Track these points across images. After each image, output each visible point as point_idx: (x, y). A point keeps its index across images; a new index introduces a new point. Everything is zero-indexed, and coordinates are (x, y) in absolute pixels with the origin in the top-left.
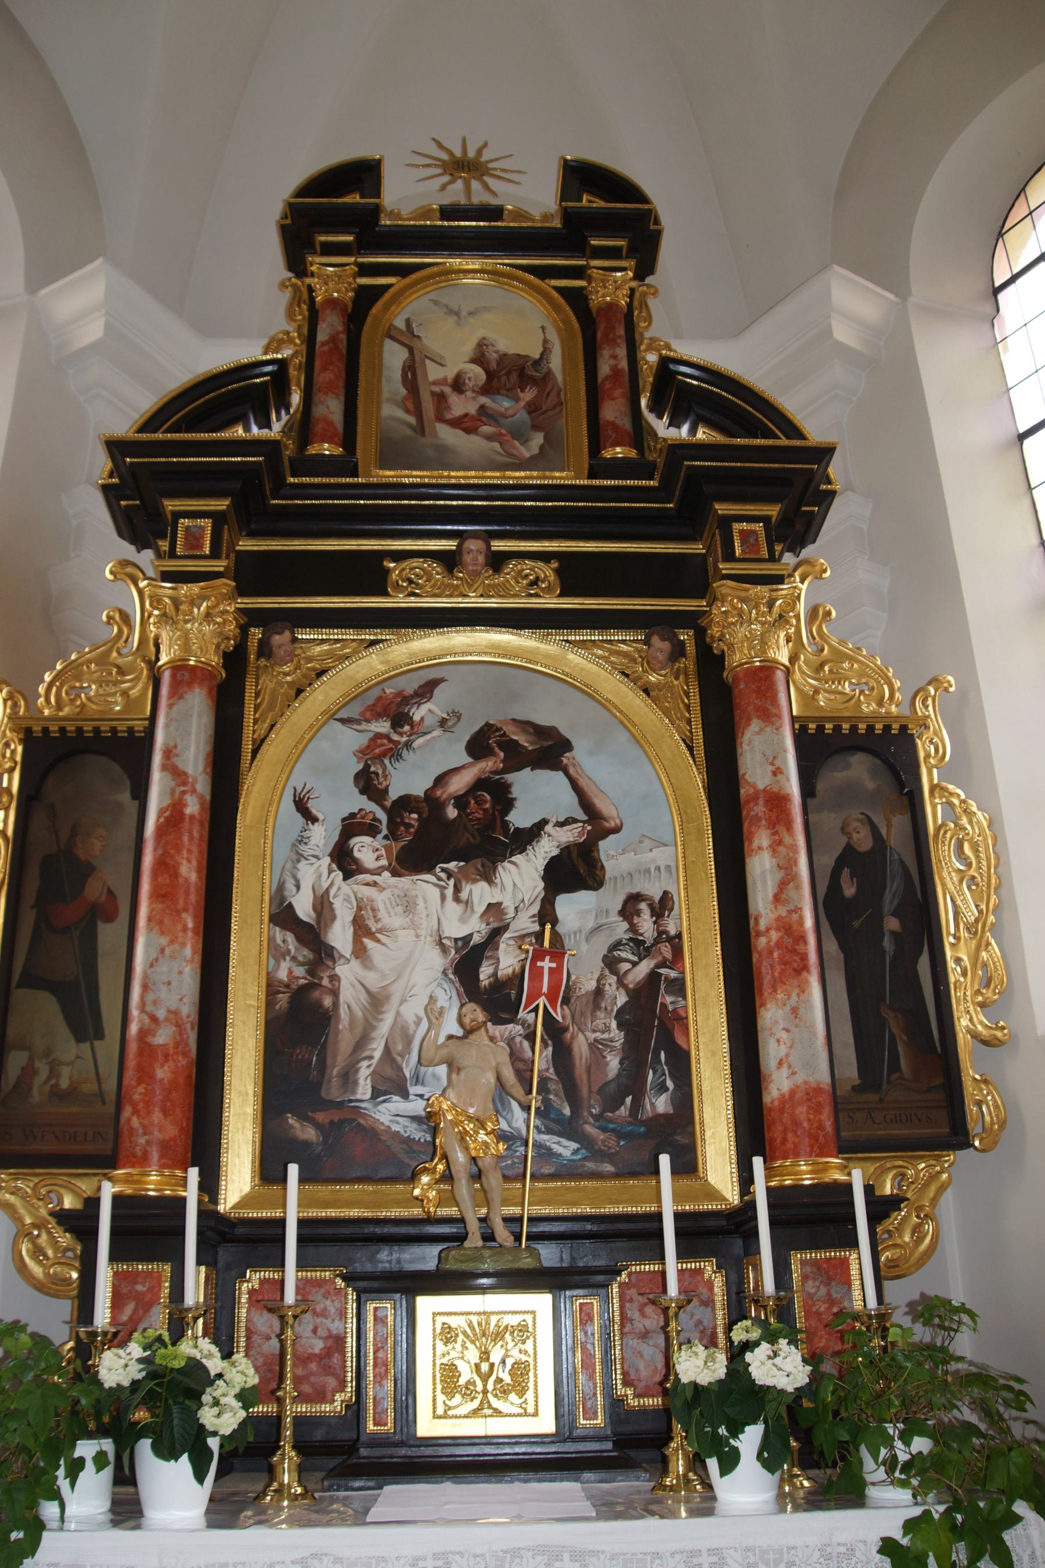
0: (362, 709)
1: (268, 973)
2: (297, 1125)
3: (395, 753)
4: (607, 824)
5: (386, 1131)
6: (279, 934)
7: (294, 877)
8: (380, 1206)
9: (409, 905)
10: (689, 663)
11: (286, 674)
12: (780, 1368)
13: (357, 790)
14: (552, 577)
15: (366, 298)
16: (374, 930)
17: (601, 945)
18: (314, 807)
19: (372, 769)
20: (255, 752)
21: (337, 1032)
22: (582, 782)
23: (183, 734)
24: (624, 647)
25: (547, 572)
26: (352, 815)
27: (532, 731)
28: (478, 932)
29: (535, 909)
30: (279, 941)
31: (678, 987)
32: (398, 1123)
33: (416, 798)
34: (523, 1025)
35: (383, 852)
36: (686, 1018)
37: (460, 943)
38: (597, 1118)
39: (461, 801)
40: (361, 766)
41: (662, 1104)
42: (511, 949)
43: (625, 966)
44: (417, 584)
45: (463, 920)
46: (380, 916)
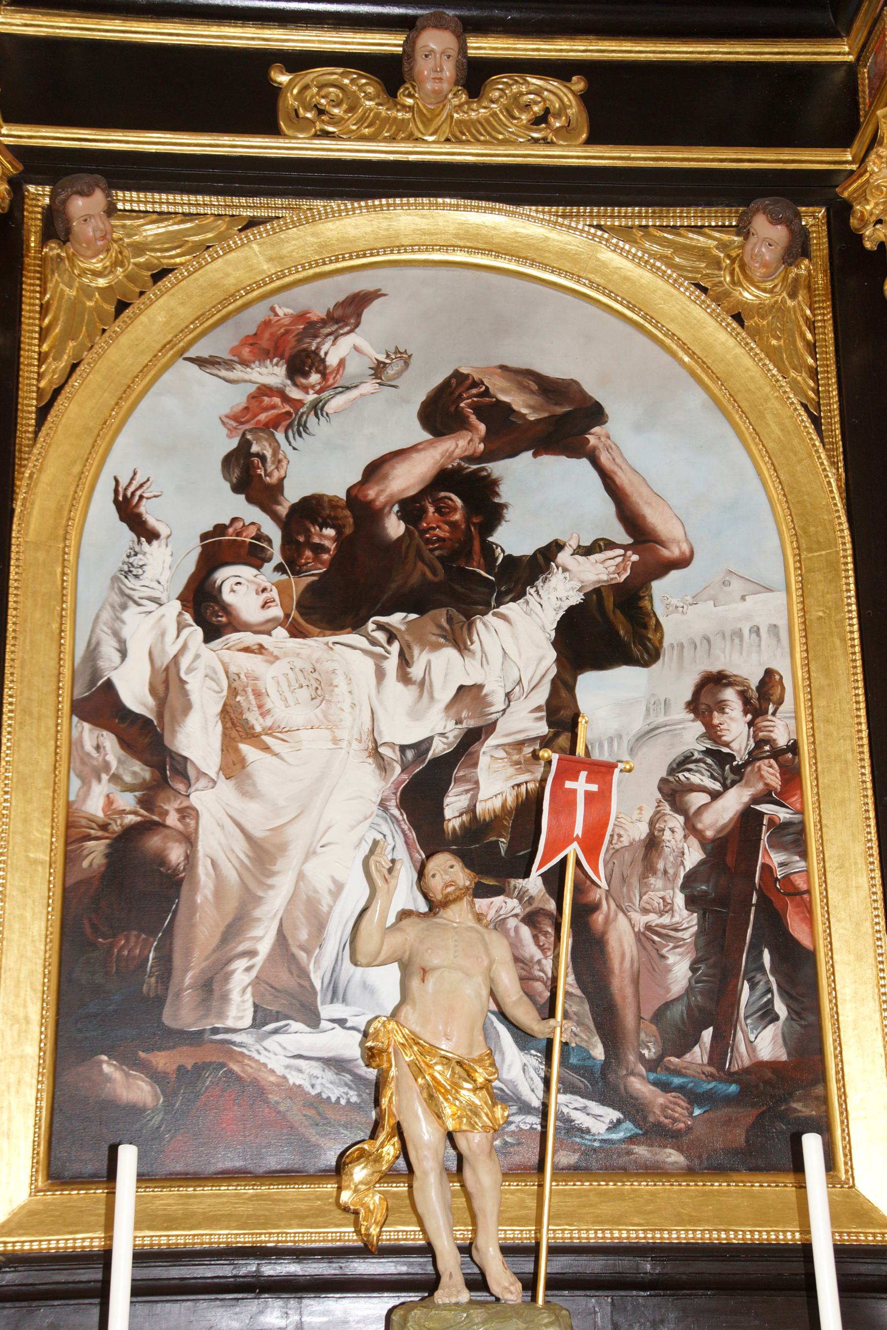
0: (236, 343)
1: (69, 805)
2: (117, 1075)
3: (294, 421)
4: (665, 553)
5: (278, 1085)
6: (88, 735)
7: (116, 634)
8: (265, 1222)
9: (320, 688)
10: (814, 269)
11: (97, 274)
13: (227, 486)
14: (574, 109)
16: (258, 729)
17: (654, 763)
18: (149, 512)
19: (255, 448)
20: (43, 413)
21: (193, 908)
22: (623, 478)
24: (700, 240)
25: (564, 96)
26: (220, 529)
27: (534, 387)
28: (442, 735)
29: (542, 696)
30: (89, 747)
31: (793, 837)
32: (300, 1071)
33: (333, 502)
34: (520, 898)
35: (275, 593)
36: (808, 892)
37: (410, 754)
38: (652, 1065)
39: (411, 509)
40: (234, 443)
41: (766, 1044)
42: (499, 764)
43: (697, 799)
44: (332, 116)
45: (415, 714)
46: (269, 705)
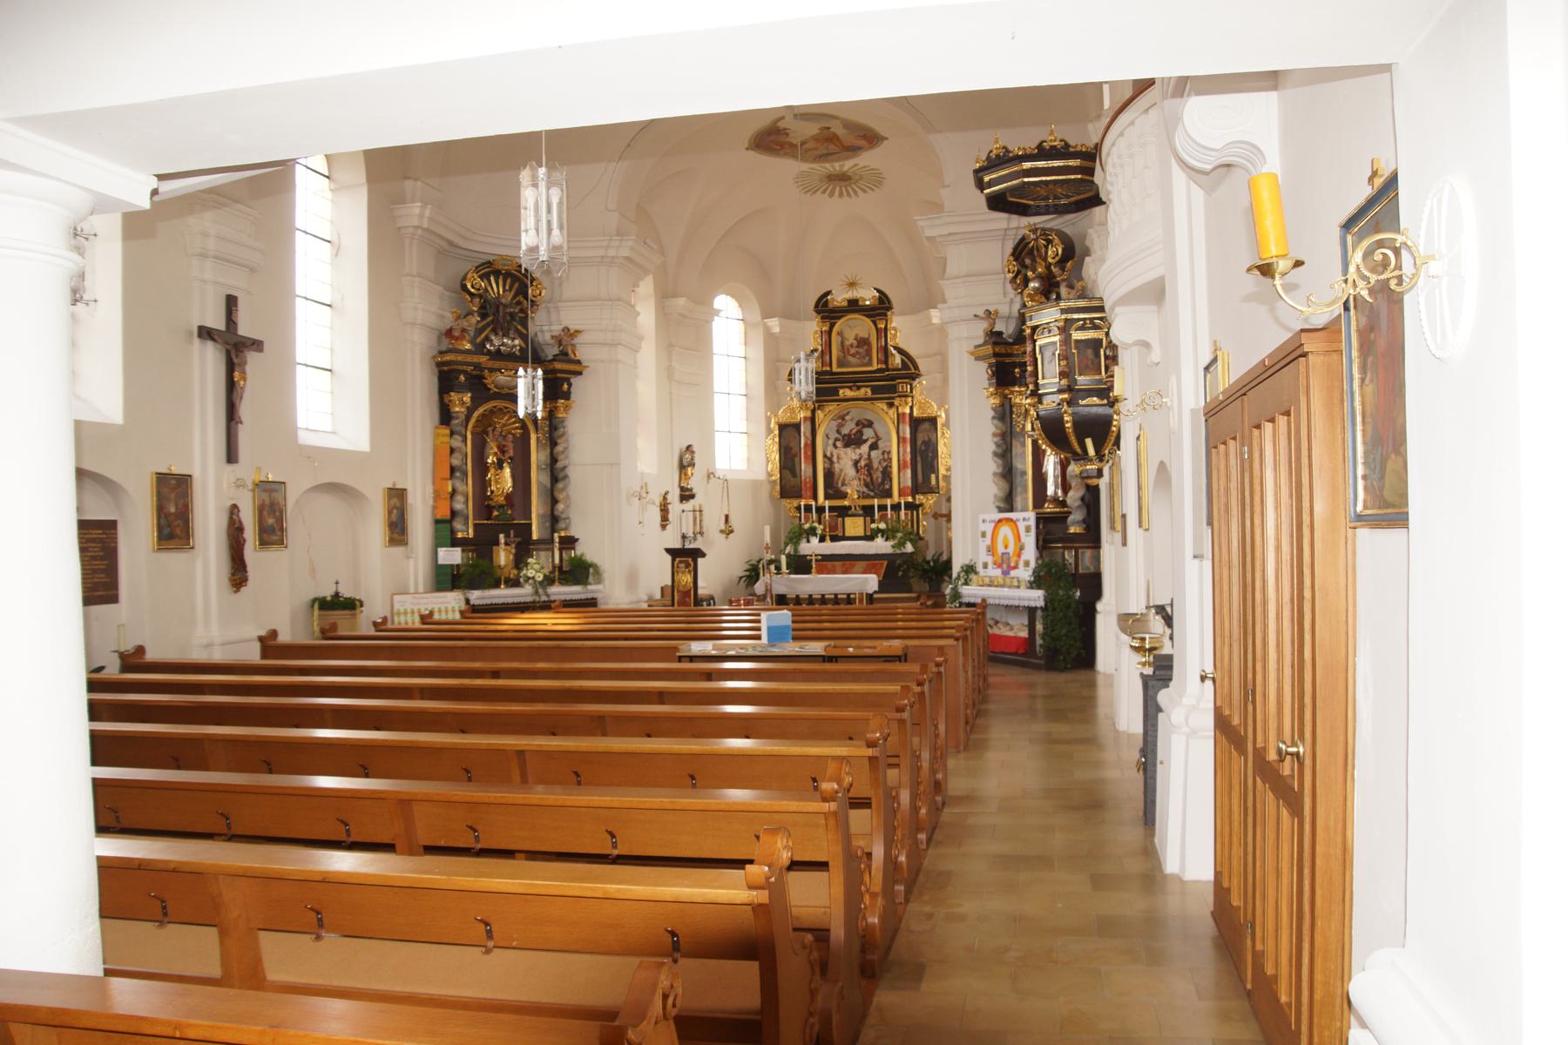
12: (882, 526)
15: (832, 326)
23: (805, 429)
